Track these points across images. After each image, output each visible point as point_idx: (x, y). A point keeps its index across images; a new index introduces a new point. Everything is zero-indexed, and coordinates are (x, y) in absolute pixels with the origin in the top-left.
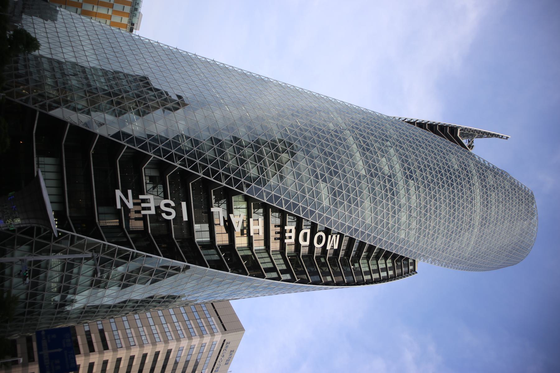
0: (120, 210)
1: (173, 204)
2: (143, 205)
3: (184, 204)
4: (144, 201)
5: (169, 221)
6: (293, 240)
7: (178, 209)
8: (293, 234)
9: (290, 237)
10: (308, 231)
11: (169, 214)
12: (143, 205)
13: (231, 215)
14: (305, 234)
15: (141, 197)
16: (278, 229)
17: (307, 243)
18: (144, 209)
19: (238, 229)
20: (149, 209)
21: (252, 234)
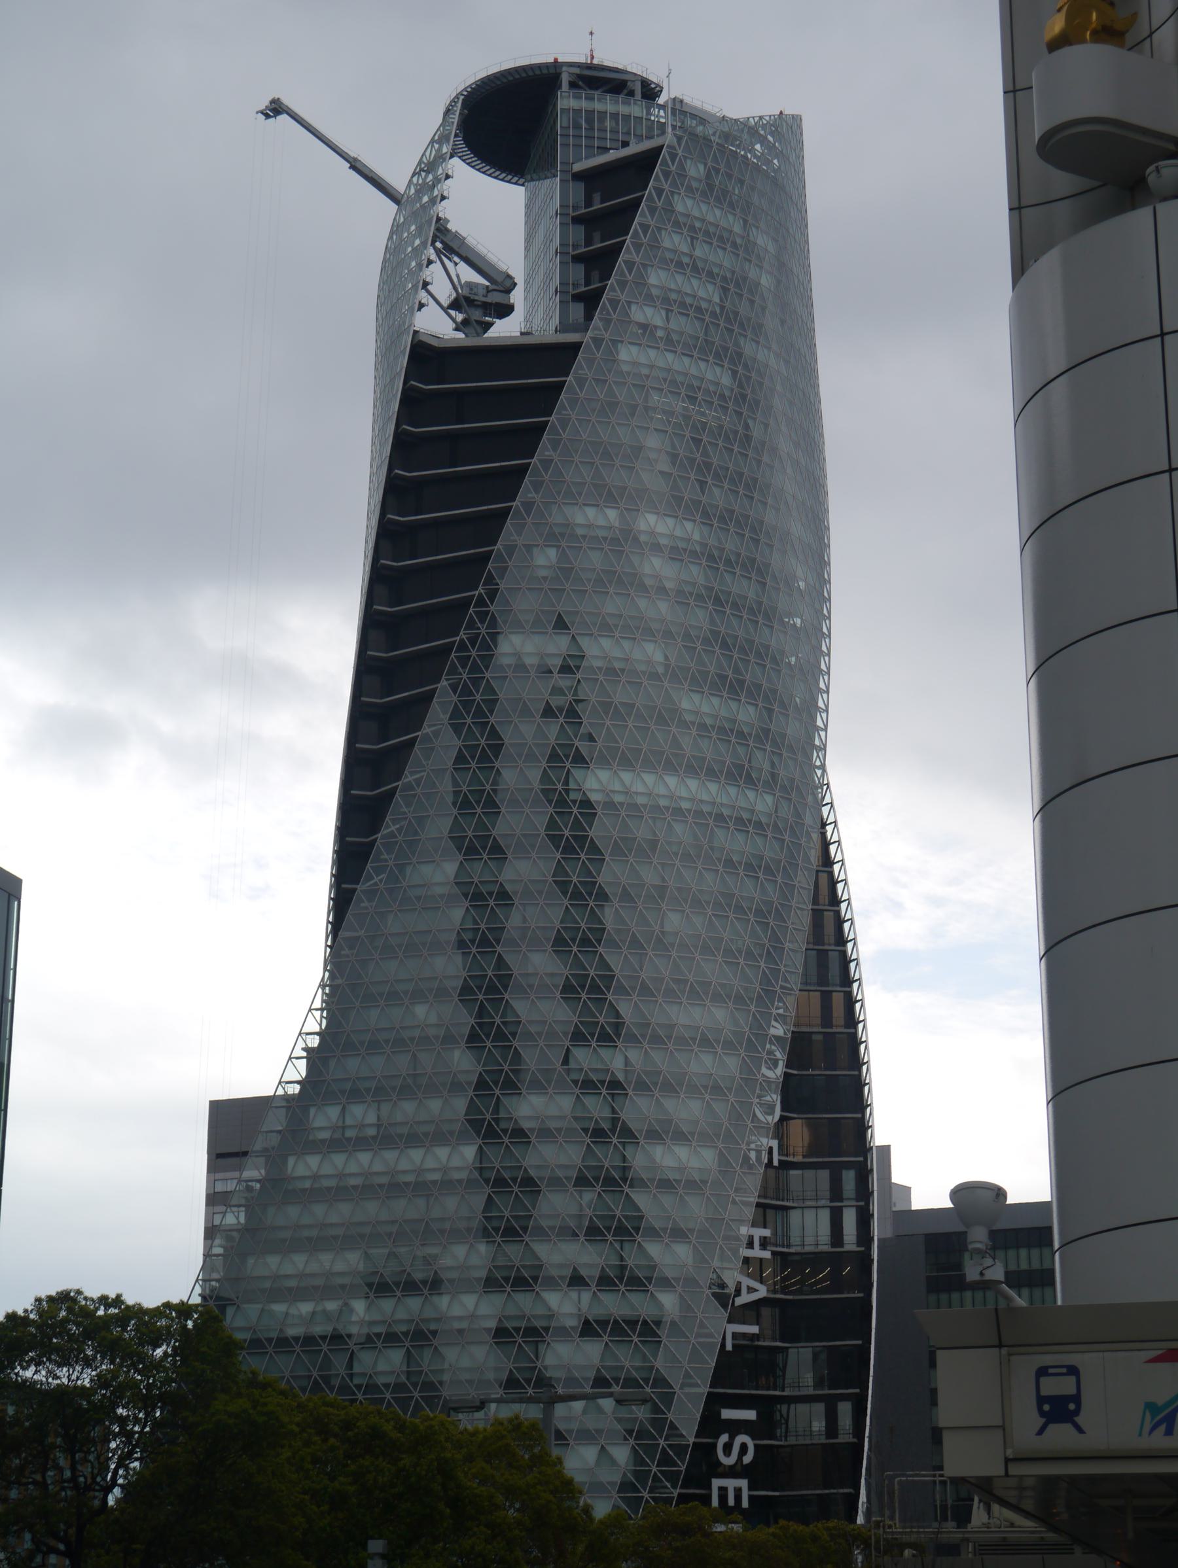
1: (724, 1438)
2: (731, 1502)
3: (727, 1414)
5: (756, 1446)
7: (735, 1427)
11: (744, 1448)
12: (731, 1502)
15: (715, 1502)
18: (738, 1497)
19: (762, 1292)
20: (738, 1491)
21: (767, 1254)
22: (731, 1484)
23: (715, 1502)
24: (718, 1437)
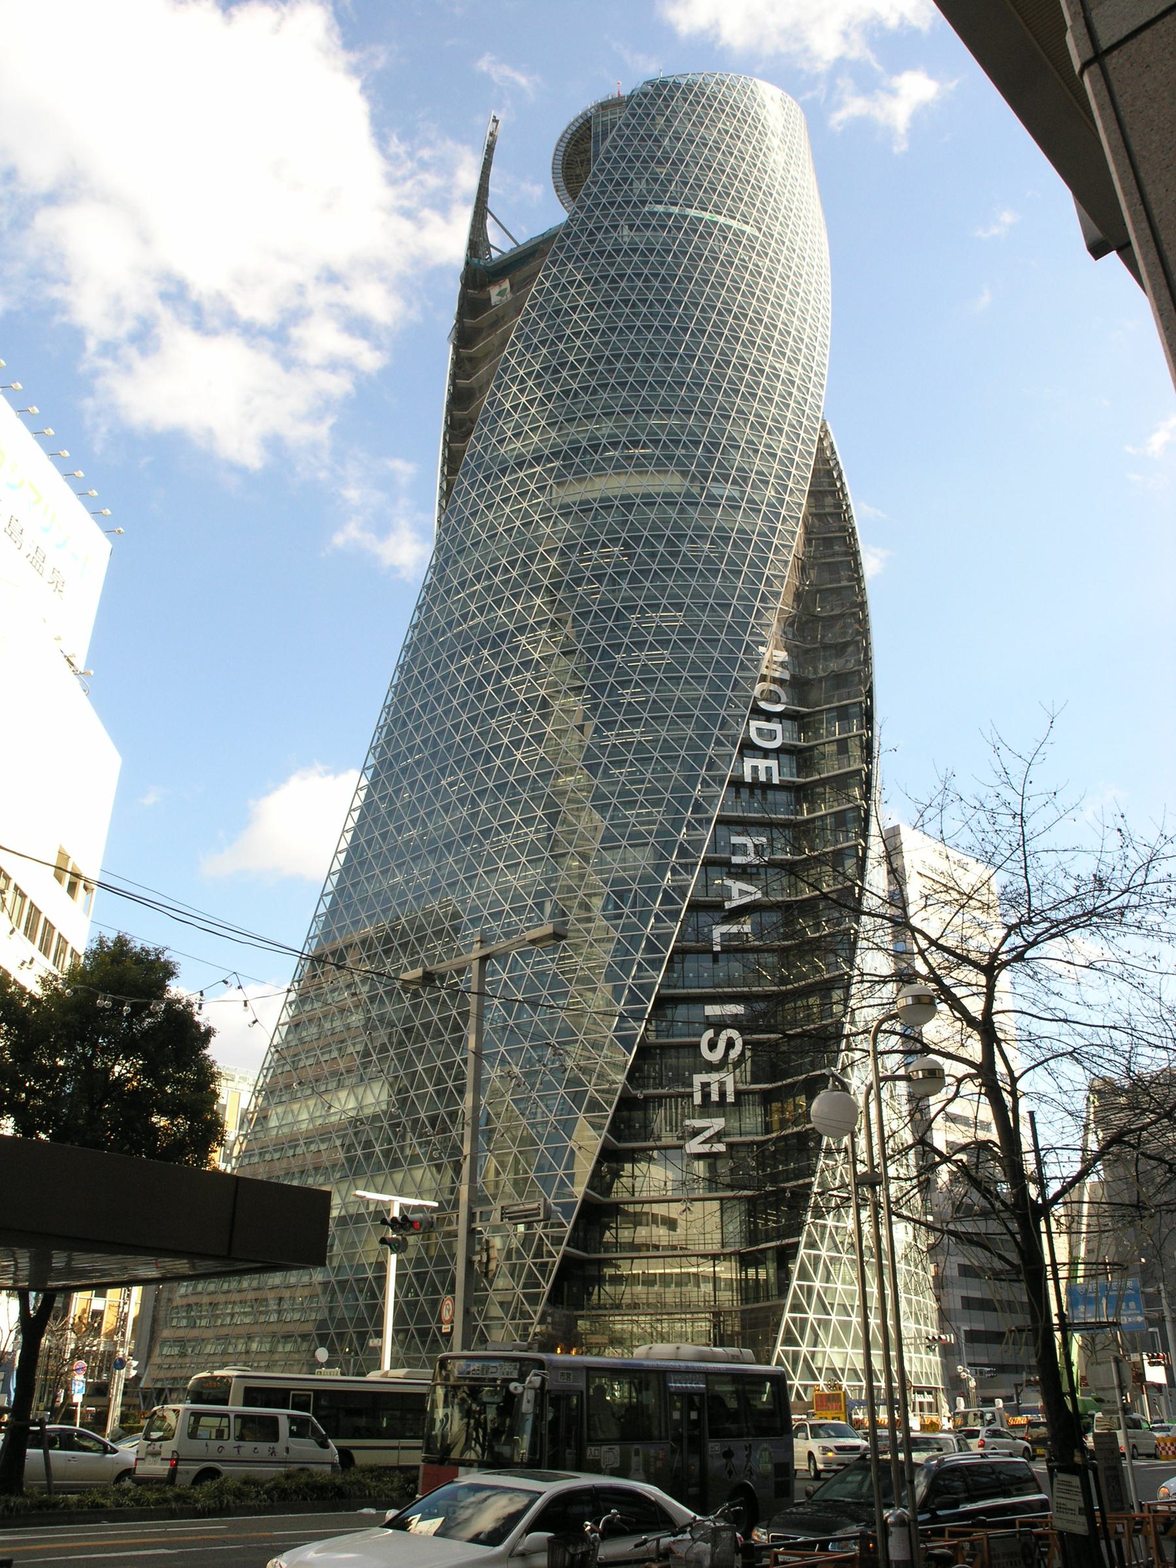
0: (730, 1146)
2: (715, 1097)
4: (706, 1096)
5: (745, 1043)
6: (773, 763)
7: (719, 1025)
8: (762, 764)
9: (768, 770)
10: (755, 724)
11: (730, 1044)
12: (715, 1097)
13: (727, 905)
14: (760, 731)
16: (745, 793)
17: (776, 726)
18: (722, 1094)
19: (754, 893)
20: (722, 1084)
22: (714, 1077)
23: (698, 1099)
24: (701, 1036)
